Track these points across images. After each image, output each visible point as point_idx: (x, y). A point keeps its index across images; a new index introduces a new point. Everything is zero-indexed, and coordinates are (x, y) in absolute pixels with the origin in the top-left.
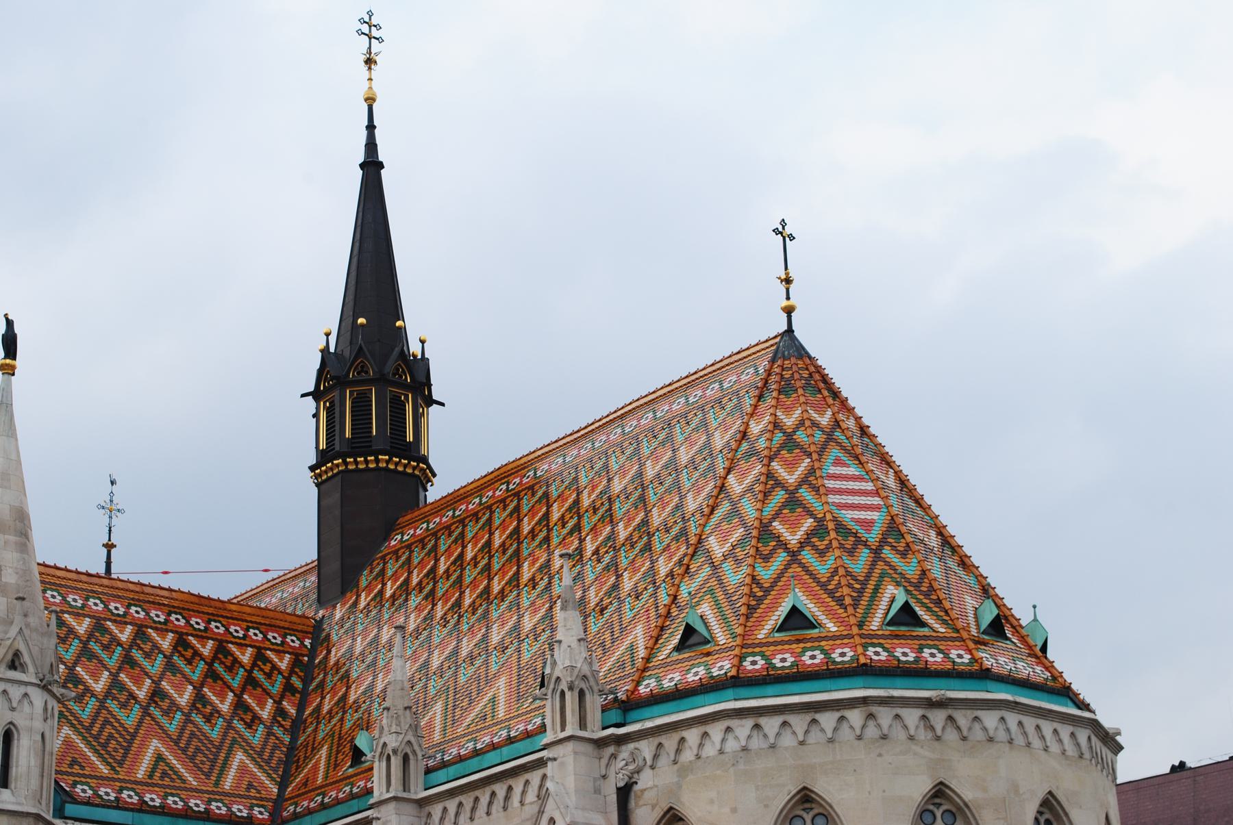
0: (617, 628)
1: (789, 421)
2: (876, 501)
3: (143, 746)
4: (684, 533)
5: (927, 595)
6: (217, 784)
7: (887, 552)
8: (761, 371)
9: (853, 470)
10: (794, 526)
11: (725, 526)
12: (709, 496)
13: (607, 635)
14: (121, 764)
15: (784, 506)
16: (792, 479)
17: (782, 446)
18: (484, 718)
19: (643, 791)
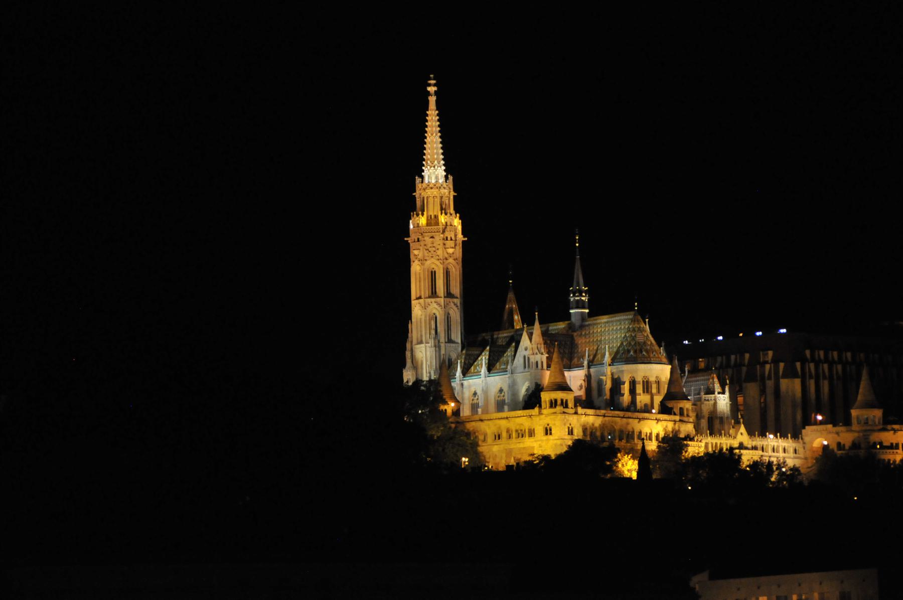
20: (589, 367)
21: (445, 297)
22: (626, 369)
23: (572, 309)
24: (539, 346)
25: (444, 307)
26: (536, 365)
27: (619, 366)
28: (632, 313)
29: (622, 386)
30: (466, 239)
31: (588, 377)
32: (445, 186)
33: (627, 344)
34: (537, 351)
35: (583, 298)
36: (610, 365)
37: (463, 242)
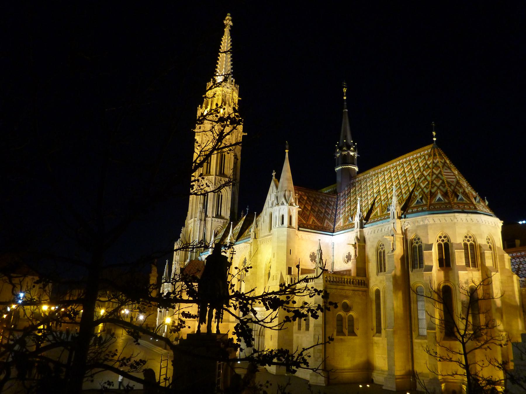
0: (402, 200)
1: (435, 161)
2: (454, 177)
3: (310, 219)
4: (415, 182)
5: (465, 195)
6: (323, 225)
7: (457, 187)
8: (429, 151)
9: (449, 171)
10: (438, 182)
11: (424, 181)
12: (420, 176)
13: (400, 201)
14: (307, 221)
15: (436, 178)
16: (437, 172)
17: (435, 166)
18: (375, 215)
19: (410, 230)
20: (362, 227)
21: (216, 175)
22: (432, 222)
23: (338, 166)
24: (287, 193)
25: (215, 184)
26: (280, 222)
27: (419, 218)
28: (431, 146)
29: (425, 252)
30: (246, 134)
31: (361, 242)
32: (229, 87)
33: (428, 184)
34: (283, 200)
35: (352, 154)
36: (400, 218)
37: (243, 136)
